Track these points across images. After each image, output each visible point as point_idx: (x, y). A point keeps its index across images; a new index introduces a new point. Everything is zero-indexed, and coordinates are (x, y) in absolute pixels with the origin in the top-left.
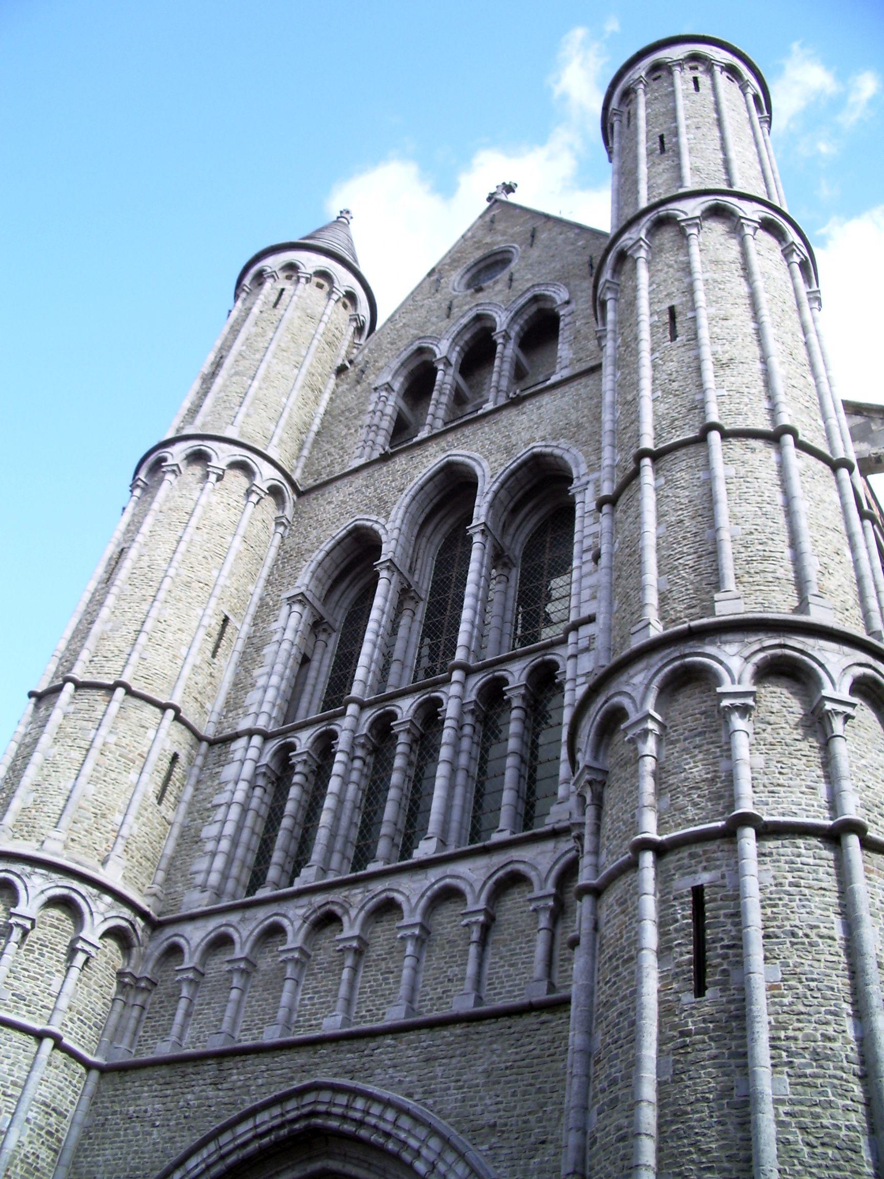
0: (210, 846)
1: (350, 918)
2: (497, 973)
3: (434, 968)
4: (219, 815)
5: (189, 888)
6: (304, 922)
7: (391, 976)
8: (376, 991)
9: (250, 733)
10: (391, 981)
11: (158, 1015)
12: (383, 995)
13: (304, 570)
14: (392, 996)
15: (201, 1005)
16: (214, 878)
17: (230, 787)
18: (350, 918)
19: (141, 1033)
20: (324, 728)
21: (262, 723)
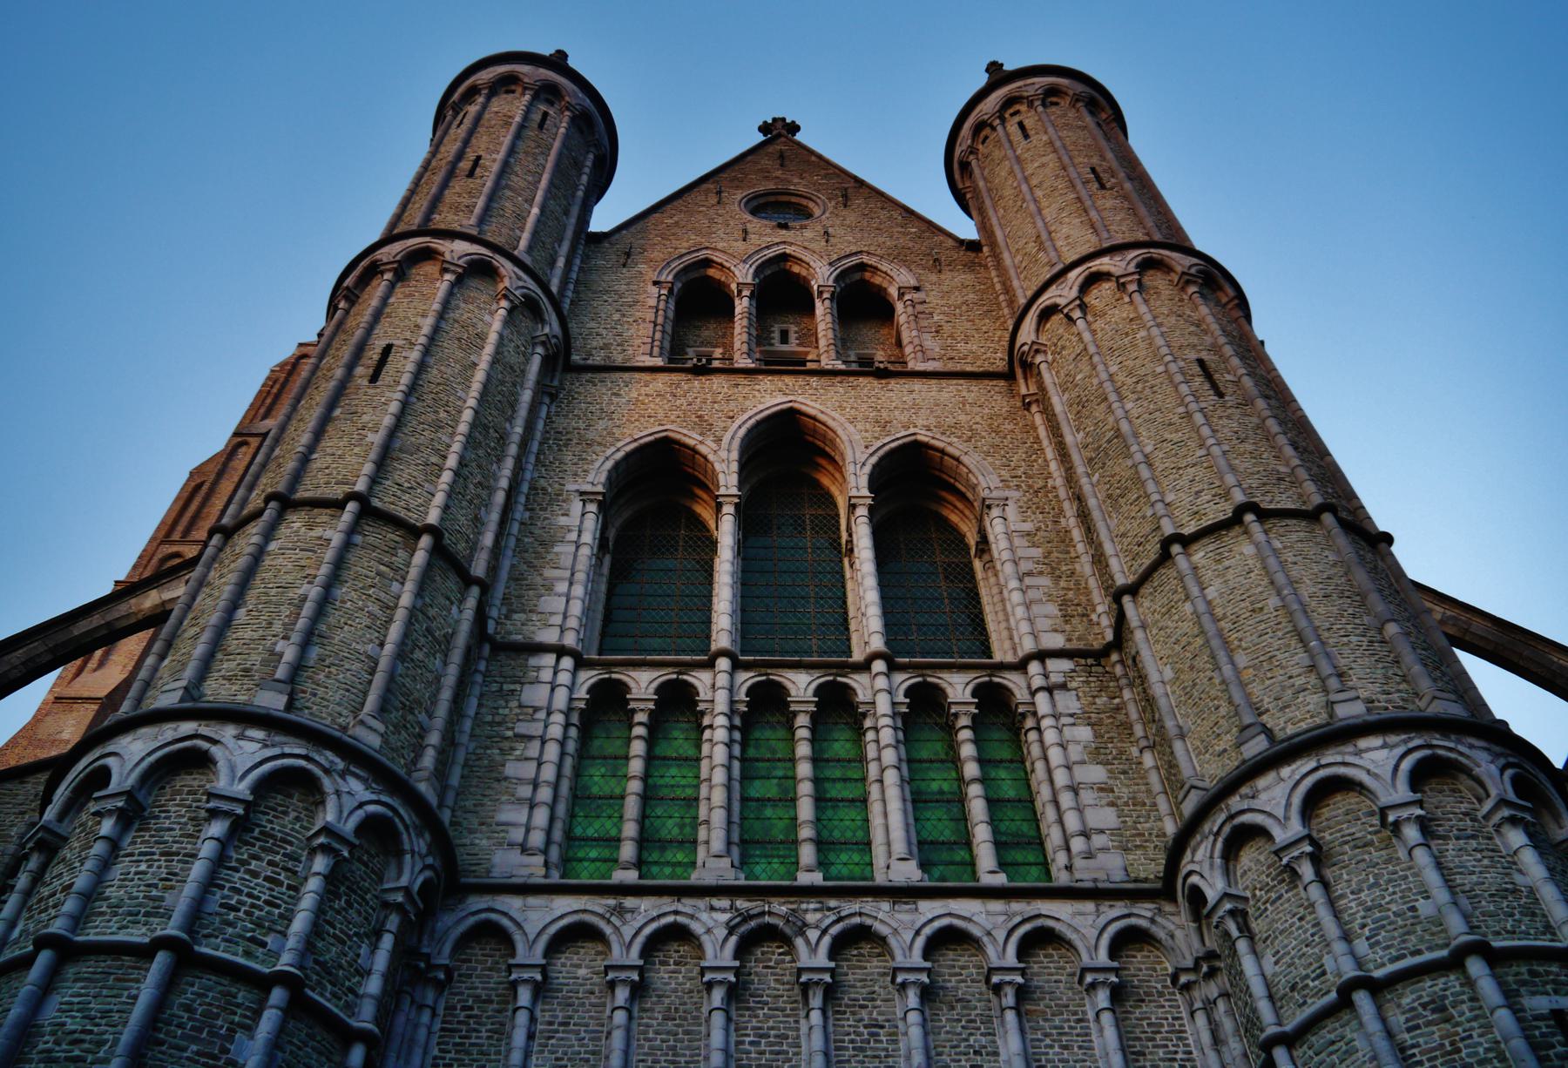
0: (525, 791)
1: (808, 942)
2: (1047, 1054)
3: (947, 1032)
4: (533, 749)
5: (501, 844)
6: (730, 934)
7: (881, 1031)
8: (862, 1049)
9: (560, 651)
10: (884, 1039)
11: (464, 1028)
12: (875, 1057)
13: (597, 464)
14: (890, 1060)
15: (551, 1023)
16: (537, 839)
17: (542, 715)
18: (808, 942)
19: (436, 1052)
20: (675, 676)
21: (570, 640)
